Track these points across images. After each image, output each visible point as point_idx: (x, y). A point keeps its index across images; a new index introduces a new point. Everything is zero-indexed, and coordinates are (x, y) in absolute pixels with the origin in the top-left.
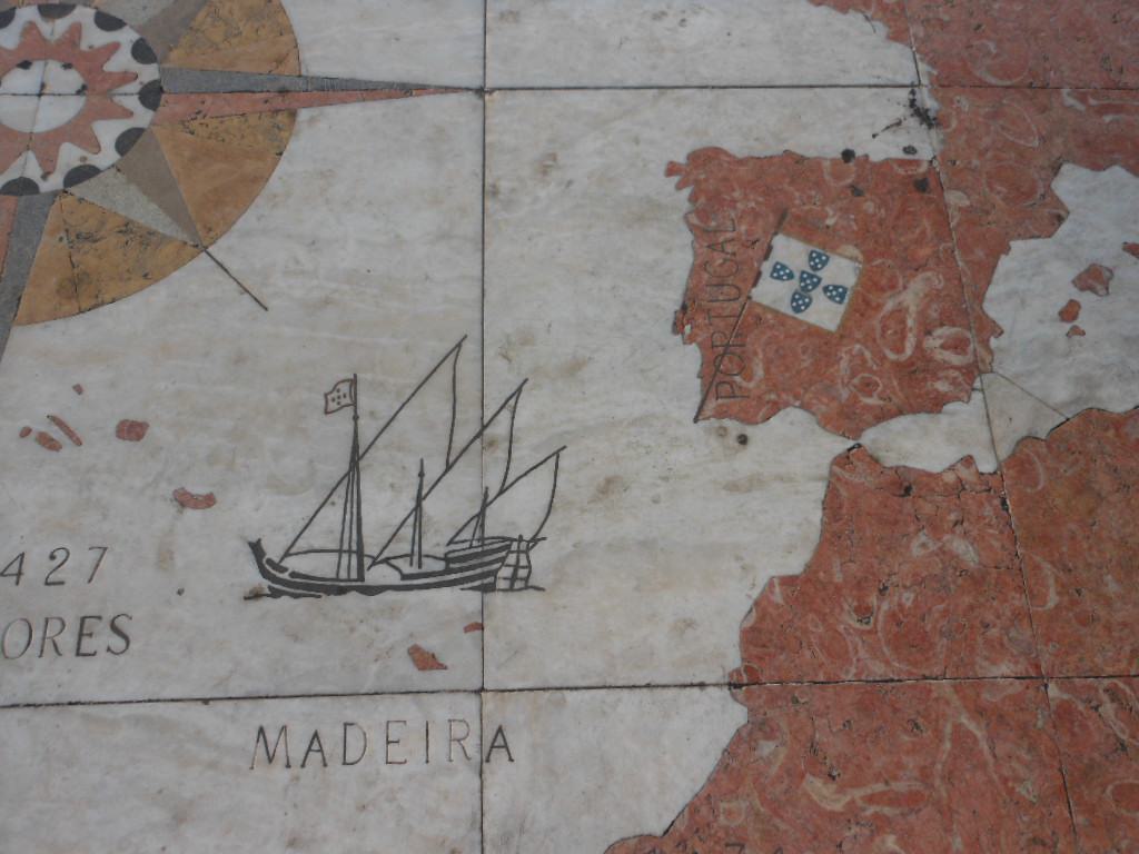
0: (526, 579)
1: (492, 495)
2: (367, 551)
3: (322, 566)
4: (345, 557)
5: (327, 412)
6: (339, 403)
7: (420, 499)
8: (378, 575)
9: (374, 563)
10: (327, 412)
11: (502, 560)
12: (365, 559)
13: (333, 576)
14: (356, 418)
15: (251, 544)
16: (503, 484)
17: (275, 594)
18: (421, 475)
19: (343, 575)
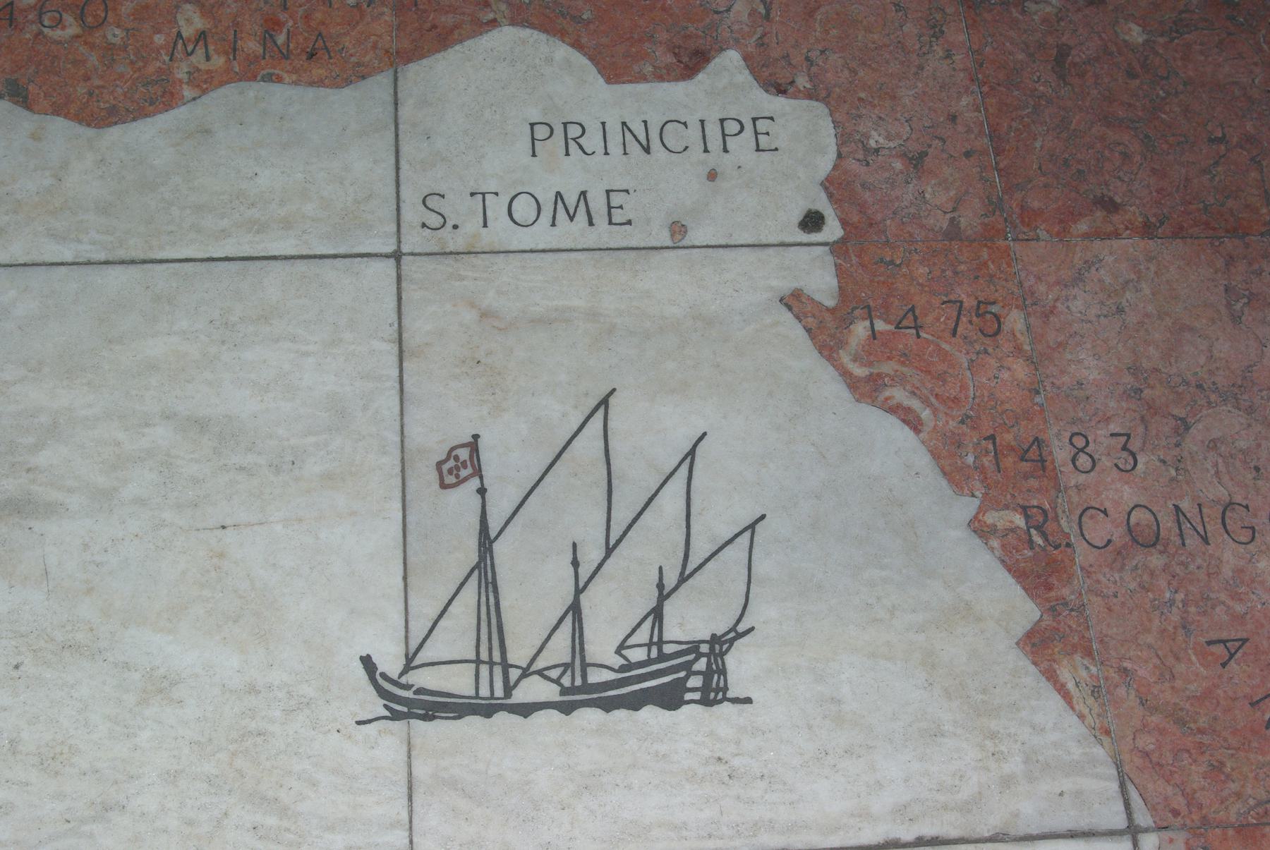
0: (725, 689)
1: (670, 582)
2: (512, 659)
3: (459, 682)
4: (484, 670)
5: (444, 486)
6: (457, 476)
7: (579, 591)
8: (534, 690)
9: (526, 673)
10: (444, 486)
11: (687, 666)
12: (511, 670)
13: (472, 693)
14: (482, 491)
15: (362, 658)
16: (684, 566)
17: (395, 716)
18: (575, 563)
19: (484, 692)
